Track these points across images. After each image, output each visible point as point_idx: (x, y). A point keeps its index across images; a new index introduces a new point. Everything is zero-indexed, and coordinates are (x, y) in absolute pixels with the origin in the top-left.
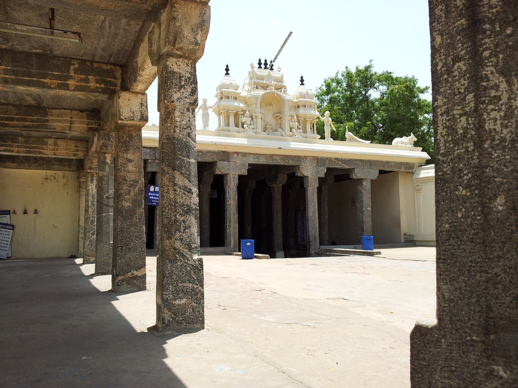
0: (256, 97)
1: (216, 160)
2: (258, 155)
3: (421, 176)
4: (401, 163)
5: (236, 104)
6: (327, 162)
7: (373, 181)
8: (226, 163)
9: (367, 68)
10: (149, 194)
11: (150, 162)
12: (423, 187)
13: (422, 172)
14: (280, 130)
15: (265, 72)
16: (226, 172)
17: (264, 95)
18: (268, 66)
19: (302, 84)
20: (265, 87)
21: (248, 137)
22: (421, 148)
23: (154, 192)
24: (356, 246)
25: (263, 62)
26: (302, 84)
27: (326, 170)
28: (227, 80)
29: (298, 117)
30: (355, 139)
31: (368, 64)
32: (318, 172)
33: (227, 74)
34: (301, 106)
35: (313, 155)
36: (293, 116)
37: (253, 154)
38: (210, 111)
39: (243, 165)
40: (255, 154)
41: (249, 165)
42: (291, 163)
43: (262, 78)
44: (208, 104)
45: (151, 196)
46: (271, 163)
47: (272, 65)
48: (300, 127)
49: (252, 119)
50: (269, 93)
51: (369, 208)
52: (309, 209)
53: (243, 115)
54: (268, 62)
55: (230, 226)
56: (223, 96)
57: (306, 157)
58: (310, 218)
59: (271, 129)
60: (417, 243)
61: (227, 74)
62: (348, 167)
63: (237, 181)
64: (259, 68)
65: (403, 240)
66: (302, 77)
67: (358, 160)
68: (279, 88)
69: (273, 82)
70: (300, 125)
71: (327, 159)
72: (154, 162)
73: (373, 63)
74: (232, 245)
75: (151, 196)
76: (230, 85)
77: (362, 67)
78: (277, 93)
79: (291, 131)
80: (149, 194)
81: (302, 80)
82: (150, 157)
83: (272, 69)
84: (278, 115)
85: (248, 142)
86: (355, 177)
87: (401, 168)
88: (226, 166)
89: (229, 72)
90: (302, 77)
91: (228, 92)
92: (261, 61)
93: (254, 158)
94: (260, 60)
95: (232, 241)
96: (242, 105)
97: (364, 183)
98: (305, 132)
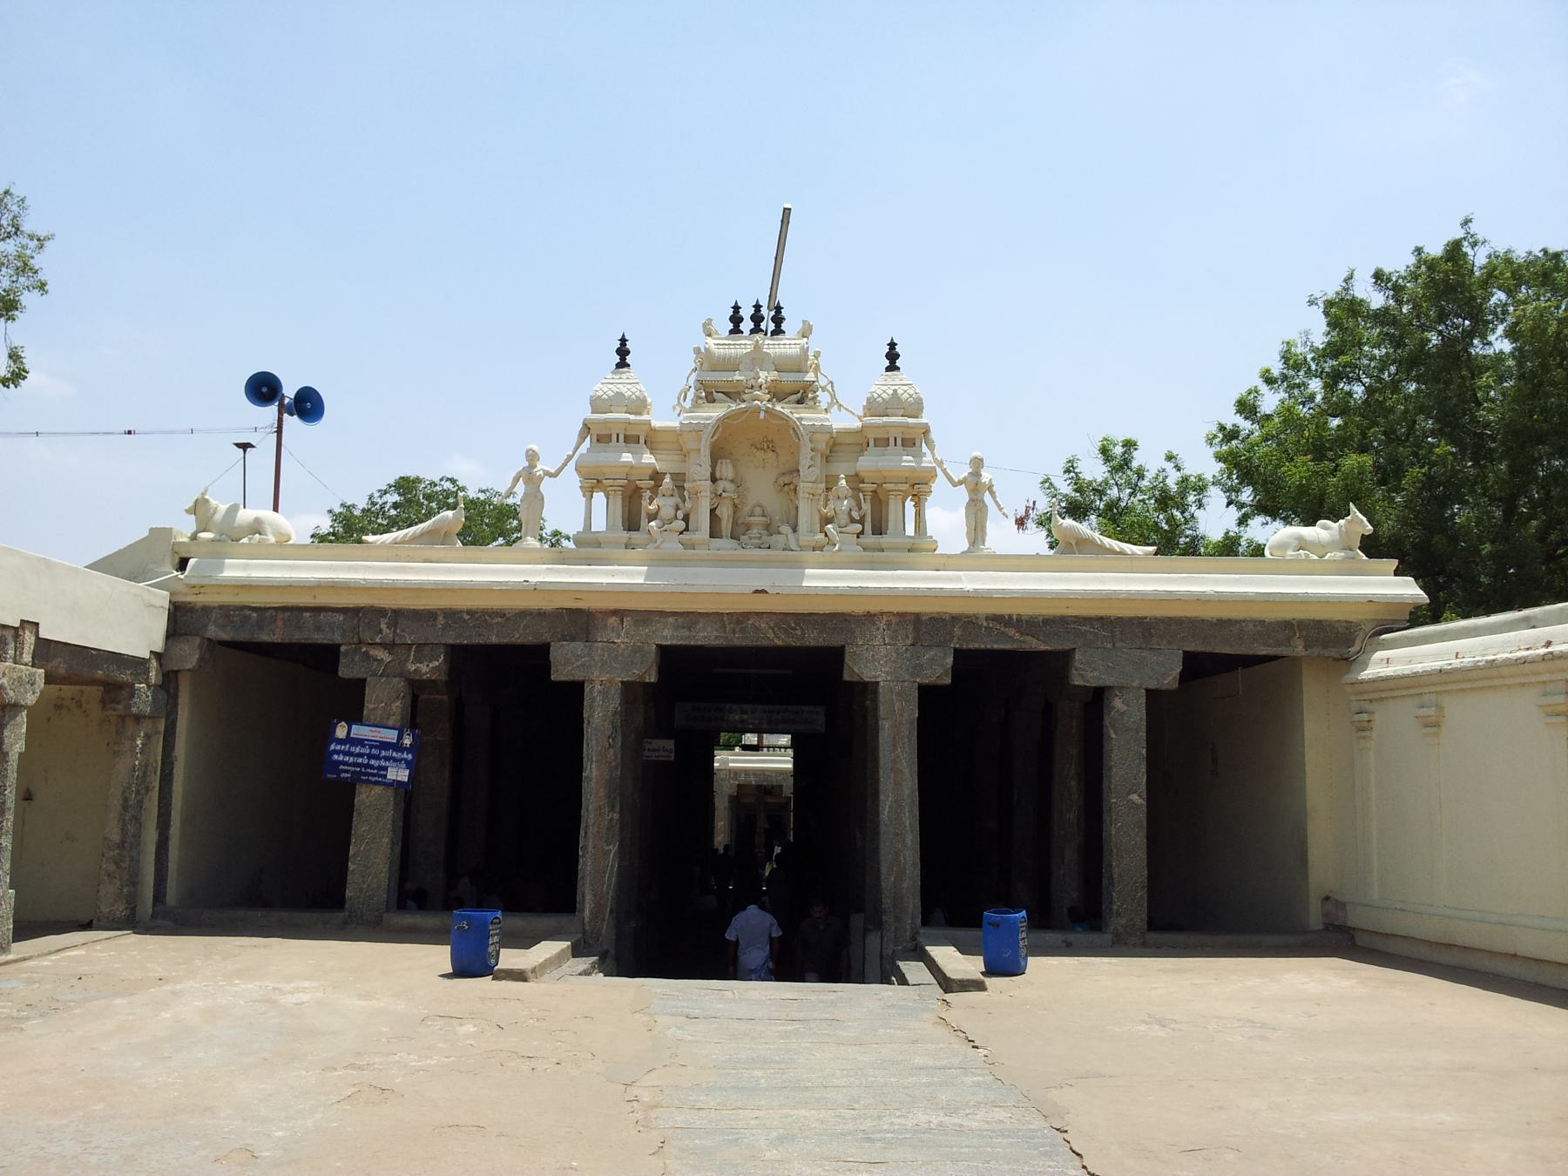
0: (697, 430)
1: (546, 637)
3: (1369, 673)
4: (1288, 625)
5: (627, 457)
6: (957, 631)
7: (1154, 697)
8: (578, 646)
9: (1454, 251)
10: (332, 747)
11: (347, 652)
12: (1376, 717)
13: (1379, 655)
14: (786, 529)
15: (744, 345)
16: (578, 677)
18: (763, 326)
19: (892, 367)
22: (1396, 562)
23: (349, 740)
24: (1071, 937)
25: (747, 312)
26: (892, 367)
27: (950, 660)
28: (607, 383)
29: (856, 480)
31: (1460, 234)
32: (917, 669)
33: (622, 364)
34: (872, 443)
35: (901, 609)
36: (836, 479)
37: (674, 614)
38: (546, 486)
39: (636, 650)
40: (682, 614)
41: (661, 648)
42: (813, 638)
43: (731, 365)
44: (541, 467)
45: (338, 752)
46: (737, 640)
47: (778, 320)
48: (856, 515)
51: (1134, 797)
52: (882, 797)
55: (585, 847)
56: (598, 435)
57: (870, 617)
58: (882, 828)
60: (1362, 940)
61: (622, 364)
62: (1043, 647)
63: (615, 703)
64: (731, 332)
65: (1315, 919)
66: (892, 345)
67: (1087, 620)
68: (778, 395)
69: (763, 374)
71: (955, 619)
72: (357, 650)
73: (1473, 228)
74: (587, 912)
75: (338, 752)
76: (618, 400)
77: (1435, 249)
80: (332, 747)
81: (892, 356)
82: (343, 636)
83: (778, 331)
84: (787, 479)
87: (1288, 642)
88: (578, 657)
89: (629, 359)
90: (892, 345)
92: (742, 312)
93: (676, 628)
94: (736, 308)
95: (588, 897)
96: (648, 458)
97: (1118, 703)
98: (879, 530)
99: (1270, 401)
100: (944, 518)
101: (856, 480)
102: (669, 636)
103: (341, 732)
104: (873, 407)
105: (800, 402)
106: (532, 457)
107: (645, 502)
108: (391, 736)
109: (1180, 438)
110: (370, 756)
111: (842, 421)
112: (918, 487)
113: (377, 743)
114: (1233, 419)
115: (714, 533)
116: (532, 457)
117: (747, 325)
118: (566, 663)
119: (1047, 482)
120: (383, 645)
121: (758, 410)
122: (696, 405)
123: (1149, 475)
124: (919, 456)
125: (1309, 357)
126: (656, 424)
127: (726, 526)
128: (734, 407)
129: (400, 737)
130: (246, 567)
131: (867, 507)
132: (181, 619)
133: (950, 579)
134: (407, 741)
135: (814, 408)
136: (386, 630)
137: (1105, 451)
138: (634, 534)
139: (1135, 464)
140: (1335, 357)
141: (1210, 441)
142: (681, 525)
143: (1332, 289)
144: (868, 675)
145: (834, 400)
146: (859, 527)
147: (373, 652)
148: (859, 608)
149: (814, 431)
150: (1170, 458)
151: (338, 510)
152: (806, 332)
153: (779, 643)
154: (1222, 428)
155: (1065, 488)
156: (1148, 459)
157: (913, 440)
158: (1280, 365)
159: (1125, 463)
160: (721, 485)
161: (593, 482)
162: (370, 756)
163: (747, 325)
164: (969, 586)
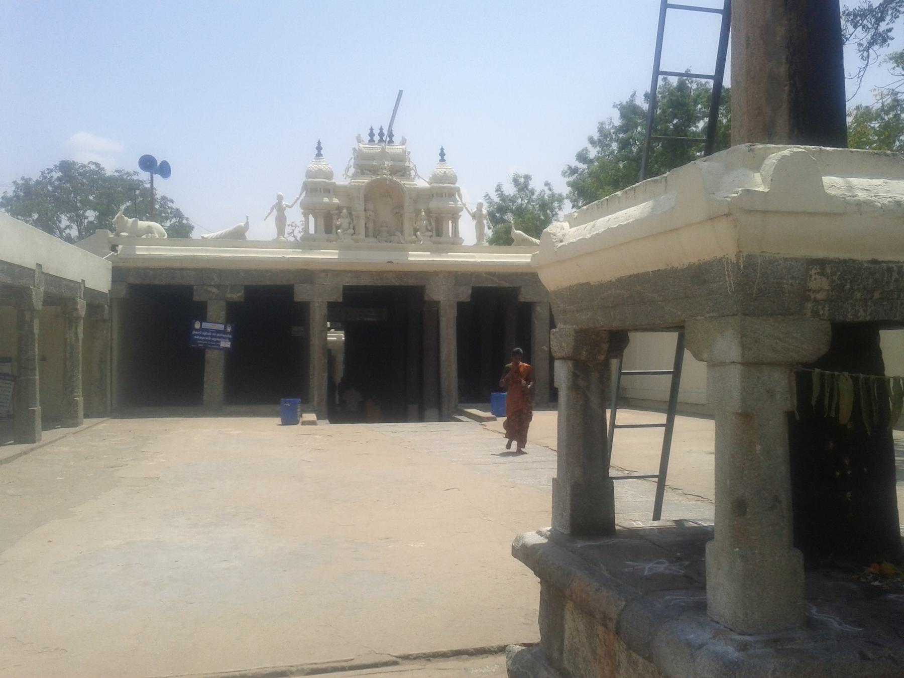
2: (357, 274)
5: (326, 200)
14: (398, 234)
17: (370, 184)
18: (384, 138)
19: (442, 160)
20: (374, 171)
21: (341, 248)
23: (201, 329)
25: (376, 132)
27: (470, 292)
28: (314, 166)
29: (428, 212)
30: (528, 240)
33: (319, 155)
37: (350, 271)
38: (287, 212)
42: (412, 282)
43: (372, 157)
46: (379, 283)
47: (391, 135)
48: (429, 228)
49: (352, 219)
50: (378, 180)
53: (339, 215)
54: (385, 132)
57: (436, 273)
59: (388, 232)
62: (508, 285)
68: (394, 171)
69: (386, 163)
70: (430, 224)
76: (319, 173)
78: (391, 180)
79: (415, 235)
83: (391, 142)
85: (339, 254)
86: (522, 300)
91: (315, 183)
92: (374, 132)
94: (372, 129)
95: (316, 396)
97: (538, 309)
98: (439, 234)
99: (593, 152)
100: (467, 230)
101: (428, 212)
102: (348, 281)
103: (197, 325)
104: (436, 179)
105: (403, 176)
106: (280, 198)
107: (334, 221)
108: (221, 327)
109: (551, 175)
110: (212, 337)
111: (422, 183)
112: (454, 216)
113: (215, 332)
114: (575, 163)
115: (367, 236)
116: (280, 198)
117: (377, 138)
118: (302, 293)
119: (487, 196)
120: (214, 286)
121: (385, 179)
122: (355, 176)
123: (537, 193)
124: (456, 201)
125: (612, 131)
126: (337, 183)
127: (371, 231)
128: (374, 178)
129: (225, 328)
130: (147, 250)
131: (433, 224)
132: (118, 274)
133: (471, 257)
134: (229, 329)
135: (409, 179)
136: (216, 279)
137: (516, 181)
138: (331, 235)
139: (530, 187)
140: (625, 132)
141: (564, 174)
142: (352, 231)
143: (625, 100)
144: (435, 298)
145: (417, 174)
146: (430, 233)
147: (210, 289)
148: (432, 269)
149: (411, 189)
150: (547, 184)
151: (20, 182)
152: (403, 142)
153: (397, 284)
154: (570, 168)
155: (496, 199)
156: (537, 185)
157: (452, 194)
158: (598, 134)
159: (526, 186)
160: (369, 213)
161: (308, 209)
162: (212, 337)
163: (377, 138)
164: (479, 260)
